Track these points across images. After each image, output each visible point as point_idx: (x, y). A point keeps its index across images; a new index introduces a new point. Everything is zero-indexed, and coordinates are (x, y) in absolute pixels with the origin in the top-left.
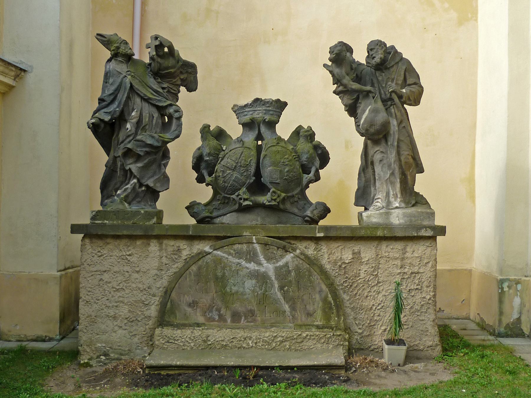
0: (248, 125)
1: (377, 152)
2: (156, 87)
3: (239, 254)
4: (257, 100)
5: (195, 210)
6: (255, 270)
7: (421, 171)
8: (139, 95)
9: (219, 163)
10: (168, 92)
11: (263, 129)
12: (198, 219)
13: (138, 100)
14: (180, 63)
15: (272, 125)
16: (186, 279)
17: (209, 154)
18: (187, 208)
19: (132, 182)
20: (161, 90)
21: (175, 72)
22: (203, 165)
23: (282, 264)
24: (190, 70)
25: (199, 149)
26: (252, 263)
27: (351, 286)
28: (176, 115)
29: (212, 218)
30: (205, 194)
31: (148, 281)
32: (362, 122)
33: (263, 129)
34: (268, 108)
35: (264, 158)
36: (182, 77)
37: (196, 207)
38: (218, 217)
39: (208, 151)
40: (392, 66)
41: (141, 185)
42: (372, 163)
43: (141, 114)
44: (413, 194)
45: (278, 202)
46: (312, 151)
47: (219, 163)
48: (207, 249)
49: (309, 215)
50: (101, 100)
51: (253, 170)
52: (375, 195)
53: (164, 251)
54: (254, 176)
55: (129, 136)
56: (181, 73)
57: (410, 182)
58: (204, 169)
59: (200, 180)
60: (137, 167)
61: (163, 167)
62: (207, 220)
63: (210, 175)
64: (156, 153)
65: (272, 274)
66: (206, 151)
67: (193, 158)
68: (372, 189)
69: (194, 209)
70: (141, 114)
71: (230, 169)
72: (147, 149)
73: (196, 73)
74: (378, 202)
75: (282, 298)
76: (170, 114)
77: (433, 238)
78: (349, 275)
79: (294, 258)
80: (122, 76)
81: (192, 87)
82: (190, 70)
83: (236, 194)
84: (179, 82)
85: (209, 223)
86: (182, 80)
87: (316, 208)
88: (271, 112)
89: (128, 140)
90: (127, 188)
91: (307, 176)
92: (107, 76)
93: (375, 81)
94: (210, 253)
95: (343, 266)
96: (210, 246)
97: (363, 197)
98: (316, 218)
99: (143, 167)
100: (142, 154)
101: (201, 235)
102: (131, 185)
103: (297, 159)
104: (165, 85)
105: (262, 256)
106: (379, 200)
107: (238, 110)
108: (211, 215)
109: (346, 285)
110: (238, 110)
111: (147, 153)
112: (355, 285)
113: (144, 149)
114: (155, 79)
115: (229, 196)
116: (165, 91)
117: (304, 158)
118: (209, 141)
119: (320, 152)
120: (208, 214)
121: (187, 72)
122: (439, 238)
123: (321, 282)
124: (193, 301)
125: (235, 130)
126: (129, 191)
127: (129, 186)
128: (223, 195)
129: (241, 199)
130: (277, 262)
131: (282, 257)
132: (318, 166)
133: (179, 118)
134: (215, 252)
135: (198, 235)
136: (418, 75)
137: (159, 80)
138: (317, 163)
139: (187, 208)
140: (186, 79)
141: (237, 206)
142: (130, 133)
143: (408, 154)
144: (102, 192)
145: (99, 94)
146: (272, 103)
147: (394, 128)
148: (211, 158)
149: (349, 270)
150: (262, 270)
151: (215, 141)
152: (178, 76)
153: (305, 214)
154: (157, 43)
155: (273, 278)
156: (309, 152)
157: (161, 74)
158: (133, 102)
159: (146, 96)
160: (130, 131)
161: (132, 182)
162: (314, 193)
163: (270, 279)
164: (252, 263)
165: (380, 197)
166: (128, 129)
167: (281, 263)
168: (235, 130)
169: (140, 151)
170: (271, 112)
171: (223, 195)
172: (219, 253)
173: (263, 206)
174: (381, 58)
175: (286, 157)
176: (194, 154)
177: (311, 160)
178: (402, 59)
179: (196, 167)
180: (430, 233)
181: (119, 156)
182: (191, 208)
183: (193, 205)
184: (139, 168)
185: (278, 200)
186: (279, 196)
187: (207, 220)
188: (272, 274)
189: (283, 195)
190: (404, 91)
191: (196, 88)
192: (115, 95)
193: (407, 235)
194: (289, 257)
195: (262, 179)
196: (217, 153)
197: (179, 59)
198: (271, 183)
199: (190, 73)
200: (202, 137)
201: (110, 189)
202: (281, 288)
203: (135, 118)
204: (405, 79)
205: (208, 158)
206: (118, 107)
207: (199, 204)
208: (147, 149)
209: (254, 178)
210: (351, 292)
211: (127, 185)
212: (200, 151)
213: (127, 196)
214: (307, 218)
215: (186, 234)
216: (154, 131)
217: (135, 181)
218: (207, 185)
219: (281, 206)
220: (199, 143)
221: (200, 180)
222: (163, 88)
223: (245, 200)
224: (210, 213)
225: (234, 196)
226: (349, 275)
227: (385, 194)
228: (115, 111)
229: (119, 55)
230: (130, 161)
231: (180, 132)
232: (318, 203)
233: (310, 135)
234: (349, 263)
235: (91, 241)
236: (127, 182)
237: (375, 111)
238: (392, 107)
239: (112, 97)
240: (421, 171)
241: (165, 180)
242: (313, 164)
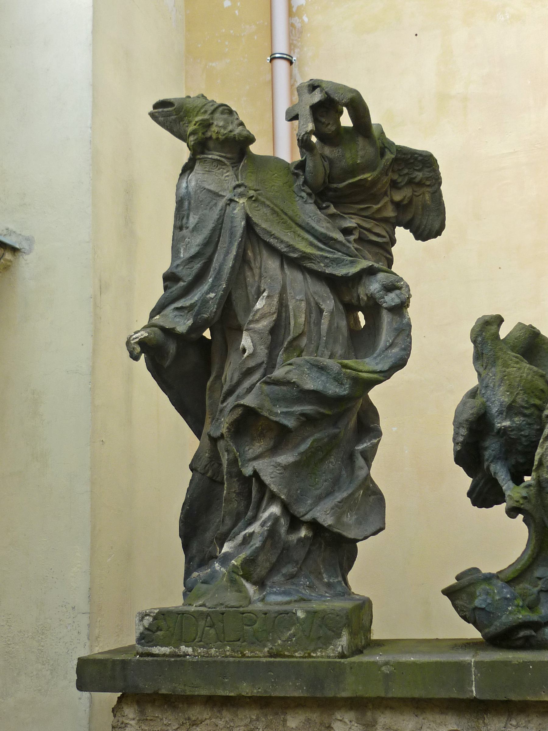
2: (323, 226)
5: (478, 602)
8: (273, 250)
10: (361, 240)
12: (492, 630)
13: (272, 265)
14: (389, 156)
17: (510, 410)
18: (449, 592)
19: (265, 515)
20: (340, 237)
21: (374, 182)
22: (492, 447)
24: (419, 175)
25: (473, 394)
28: (391, 299)
29: (537, 626)
36: (397, 197)
37: (479, 590)
39: (506, 400)
41: (295, 523)
43: (282, 305)
50: (170, 278)
55: (249, 372)
56: (394, 185)
58: (496, 459)
60: (279, 464)
61: (360, 461)
62: (522, 634)
63: (517, 480)
64: (335, 420)
66: (500, 398)
67: (457, 425)
69: (472, 596)
70: (282, 305)
72: (308, 408)
73: (437, 180)
76: (371, 298)
80: (222, 203)
81: (428, 223)
82: (419, 175)
84: (390, 213)
85: (528, 645)
86: (398, 205)
89: (246, 384)
90: (252, 534)
92: (183, 207)
99: (296, 465)
100: (290, 423)
101: (514, 697)
102: (263, 525)
104: (351, 223)
108: (534, 617)
111: (308, 421)
113: (298, 409)
114: (320, 208)
116: (352, 238)
118: (506, 365)
120: (523, 616)
121: (411, 182)
126: (257, 543)
127: (255, 528)
133: (400, 309)
135: (501, 697)
137: (332, 210)
139: (449, 592)
140: (411, 201)
142: (251, 363)
144: (186, 547)
145: (165, 264)
148: (518, 420)
151: (526, 365)
152: (385, 194)
154: (317, 97)
157: (336, 190)
158: (256, 271)
159: (295, 250)
160: (251, 356)
161: (265, 515)
166: (244, 350)
169: (285, 415)
176: (458, 413)
179: (469, 455)
181: (222, 436)
182: (462, 592)
183: (472, 584)
184: (285, 468)
187: (522, 634)
191: (442, 227)
192: (205, 256)
196: (537, 402)
197: (384, 146)
199: (420, 184)
200: (478, 357)
201: (209, 535)
203: (263, 317)
205: (507, 423)
206: (211, 290)
207: (489, 578)
208: (308, 408)
211: (250, 523)
212: (478, 401)
213: (250, 562)
215: (455, 694)
216: (327, 353)
217: (275, 509)
218: (512, 512)
220: (472, 381)
222: (346, 232)
224: (532, 607)
228: (204, 302)
229: (211, 144)
230: (258, 447)
231: (407, 349)
235: (142, 712)
236: (250, 514)
239: (197, 266)
241: (371, 502)
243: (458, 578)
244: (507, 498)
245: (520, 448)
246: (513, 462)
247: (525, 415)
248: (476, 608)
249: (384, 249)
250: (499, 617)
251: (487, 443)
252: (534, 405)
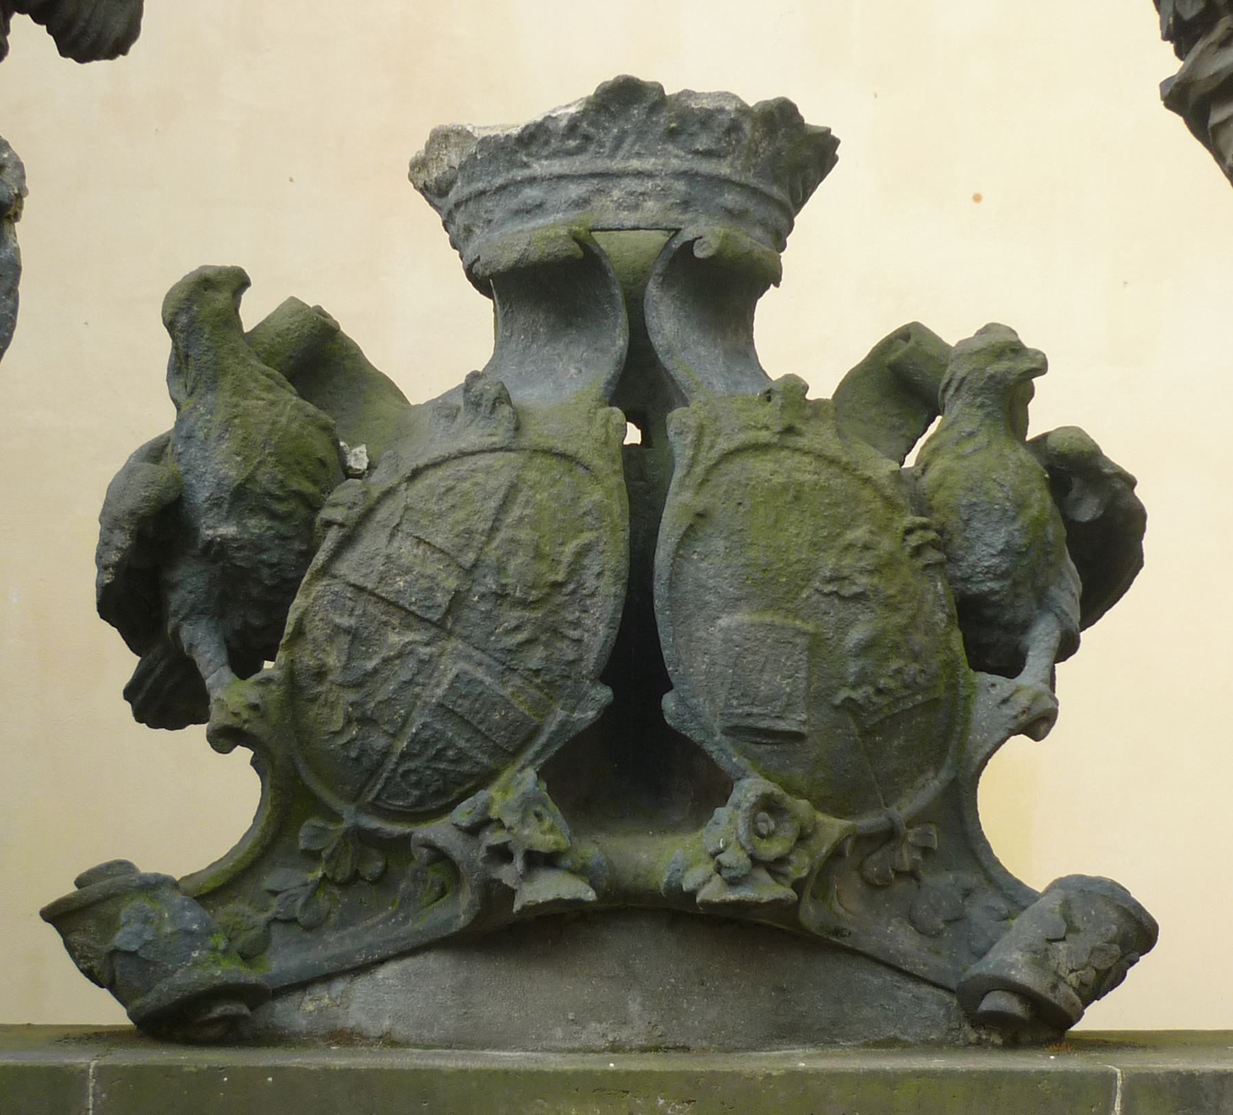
0: (542, 291)
4: (623, 97)
5: (121, 939)
9: (324, 571)
11: (667, 324)
12: (149, 1001)
15: (728, 287)
17: (240, 498)
18: (60, 916)
22: (188, 583)
25: (156, 452)
29: (257, 996)
30: (194, 803)
33: (667, 324)
34: (706, 167)
35: (688, 536)
37: (127, 910)
38: (303, 985)
39: (233, 473)
45: (798, 886)
46: (1040, 501)
47: (324, 571)
49: (1024, 975)
51: (597, 626)
54: (605, 676)
58: (195, 612)
59: (164, 698)
62: (218, 1011)
63: (243, 663)
66: (217, 467)
67: (110, 522)
69: (110, 925)
71: (411, 618)
83: (463, 814)
85: (233, 1034)
87: (1072, 929)
88: (730, 199)
91: (1003, 685)
98: (1064, 995)
103: (933, 556)
107: (464, 180)
108: (251, 976)
110: (464, 180)
115: (397, 829)
117: (987, 548)
118: (241, 391)
119: (1088, 511)
120: (226, 971)
125: (427, 328)
128: (350, 816)
129: (502, 854)
132: (1076, 617)
139: (60, 916)
141: (460, 910)
146: (734, 128)
148: (257, 525)
151: (289, 397)
153: (977, 969)
156: (1021, 506)
162: (1040, 811)
168: (427, 328)
170: (730, 199)
171: (346, 828)
173: (674, 911)
175: (859, 534)
176: (115, 492)
177: (1027, 569)
179: (134, 593)
182: (89, 917)
183: (113, 897)
185: (800, 866)
186: (803, 838)
187: (218, 1011)
189: (833, 827)
195: (669, 702)
196: (307, 487)
198: (740, 732)
200: (179, 365)
205: (228, 530)
207: (155, 886)
209: (604, 694)
212: (163, 472)
214: (996, 1002)
218: (224, 739)
219: (810, 914)
220: (158, 416)
221: (164, 698)
223: (539, 861)
224: (248, 957)
225: (440, 831)
242: (1043, 600)
243: (80, 883)
244: (213, 707)
245: (255, 591)
246: (237, 624)
247: (273, 515)
248: (115, 952)
250: (168, 974)
251: (177, 575)
252: (299, 495)
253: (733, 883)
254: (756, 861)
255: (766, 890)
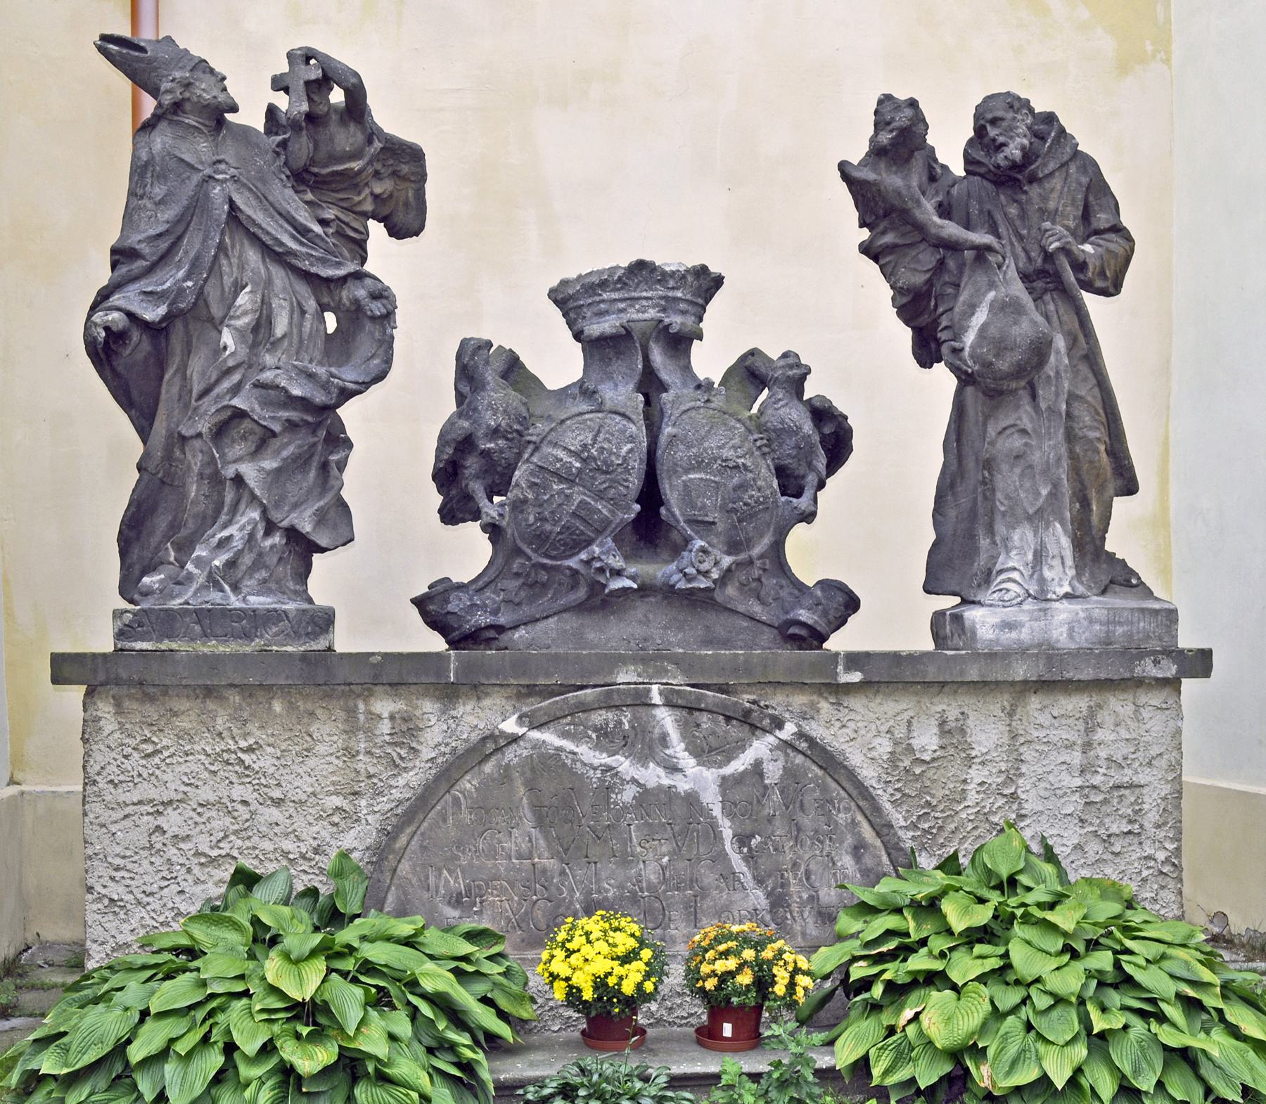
1: (1008, 432)
2: (303, 216)
3: (606, 738)
6: (660, 788)
7: (1130, 487)
8: (255, 239)
9: (527, 460)
10: (339, 234)
11: (658, 357)
13: (253, 256)
14: (378, 145)
15: (680, 343)
16: (445, 820)
19: (244, 520)
20: (317, 229)
21: (360, 172)
22: (472, 464)
23: (742, 768)
24: (405, 169)
26: (651, 765)
27: (940, 828)
28: (377, 308)
29: (500, 629)
31: (315, 829)
32: (970, 338)
33: (658, 357)
34: (670, 294)
35: (670, 443)
36: (378, 190)
40: (1052, 174)
41: (270, 528)
42: (988, 465)
43: (265, 303)
44: (1104, 557)
45: (715, 581)
47: (527, 460)
48: (510, 726)
52: (994, 558)
53: (361, 735)
54: (638, 502)
55: (229, 372)
56: (377, 175)
57: (1095, 518)
58: (477, 477)
60: (263, 469)
61: (335, 471)
64: (314, 428)
65: (711, 798)
68: (984, 542)
69: (447, 601)
70: (265, 303)
71: (562, 479)
72: (294, 415)
73: (423, 177)
74: (1010, 580)
75: (745, 869)
76: (356, 302)
77: (1173, 684)
78: (933, 796)
79: (777, 748)
80: (196, 178)
81: (406, 224)
82: (405, 169)
83: (583, 556)
84: (368, 206)
86: (376, 197)
88: (682, 306)
89: (226, 384)
90: (230, 538)
92: (141, 171)
93: (999, 217)
94: (515, 739)
95: (918, 771)
96: (520, 718)
97: (956, 562)
99: (278, 471)
100: (277, 428)
102: (242, 529)
103: (766, 450)
104: (330, 214)
105: (683, 745)
106: (1015, 575)
107: (570, 300)
109: (926, 826)
110: (570, 300)
111: (291, 426)
112: (953, 826)
113: (285, 414)
114: (296, 192)
115: (554, 563)
116: (331, 231)
121: (395, 174)
122: (1186, 683)
123: (860, 818)
124: (469, 889)
125: (557, 361)
126: (237, 544)
127: (232, 530)
128: (537, 559)
130: (729, 760)
131: (741, 747)
134: (535, 734)
136: (1117, 204)
137: (309, 196)
138: (821, 462)
140: (391, 196)
141: (582, 593)
142: (231, 363)
143: (1099, 439)
144: (123, 553)
146: (684, 277)
147: (1059, 361)
149: (934, 781)
150: (683, 786)
152: (367, 184)
154: (315, 74)
155: (717, 811)
157: (315, 175)
158: (235, 261)
159: (281, 244)
160: (233, 354)
161: (244, 520)
163: (706, 812)
164: (651, 765)
165: (1016, 565)
166: (225, 348)
167: (739, 765)
168: (557, 361)
169: (273, 418)
170: (682, 306)
171: (535, 560)
172: (549, 737)
173: (668, 592)
174: (1023, 148)
175: (736, 441)
178: (1077, 154)
180: (1170, 670)
181: (199, 435)
184: (269, 473)
185: (715, 575)
186: (716, 563)
188: (711, 798)
190: (1088, 248)
191: (422, 228)
193: (1103, 676)
194: (760, 748)
195: (663, 511)
197: (373, 133)
198: (692, 522)
199: (404, 178)
201: (154, 541)
202: (742, 840)
203: (245, 313)
204: (1086, 216)
206: (188, 277)
207: (461, 587)
208: (294, 415)
209: (637, 507)
210: (943, 845)
211: (225, 526)
213: (231, 564)
216: (307, 358)
217: (256, 515)
222: (323, 223)
225: (572, 563)
226: (933, 796)
227: (1030, 557)
228: (181, 292)
229: (188, 107)
230: (239, 449)
231: (388, 361)
232: (825, 584)
233: (793, 376)
234: (934, 760)
236: (223, 518)
237: (1007, 308)
238: (1047, 297)
239: (164, 245)
240: (1130, 487)
243: (429, 587)
244: (484, 516)
245: (499, 469)
246: (490, 482)
247: (507, 439)
248: (448, 613)
249: (359, 247)
250: (468, 621)
251: (468, 463)
252: (517, 431)
253: (689, 581)
254: (699, 572)
255: (703, 584)
